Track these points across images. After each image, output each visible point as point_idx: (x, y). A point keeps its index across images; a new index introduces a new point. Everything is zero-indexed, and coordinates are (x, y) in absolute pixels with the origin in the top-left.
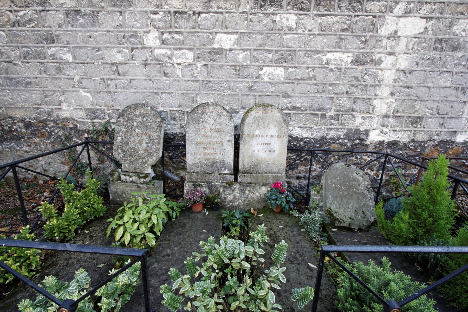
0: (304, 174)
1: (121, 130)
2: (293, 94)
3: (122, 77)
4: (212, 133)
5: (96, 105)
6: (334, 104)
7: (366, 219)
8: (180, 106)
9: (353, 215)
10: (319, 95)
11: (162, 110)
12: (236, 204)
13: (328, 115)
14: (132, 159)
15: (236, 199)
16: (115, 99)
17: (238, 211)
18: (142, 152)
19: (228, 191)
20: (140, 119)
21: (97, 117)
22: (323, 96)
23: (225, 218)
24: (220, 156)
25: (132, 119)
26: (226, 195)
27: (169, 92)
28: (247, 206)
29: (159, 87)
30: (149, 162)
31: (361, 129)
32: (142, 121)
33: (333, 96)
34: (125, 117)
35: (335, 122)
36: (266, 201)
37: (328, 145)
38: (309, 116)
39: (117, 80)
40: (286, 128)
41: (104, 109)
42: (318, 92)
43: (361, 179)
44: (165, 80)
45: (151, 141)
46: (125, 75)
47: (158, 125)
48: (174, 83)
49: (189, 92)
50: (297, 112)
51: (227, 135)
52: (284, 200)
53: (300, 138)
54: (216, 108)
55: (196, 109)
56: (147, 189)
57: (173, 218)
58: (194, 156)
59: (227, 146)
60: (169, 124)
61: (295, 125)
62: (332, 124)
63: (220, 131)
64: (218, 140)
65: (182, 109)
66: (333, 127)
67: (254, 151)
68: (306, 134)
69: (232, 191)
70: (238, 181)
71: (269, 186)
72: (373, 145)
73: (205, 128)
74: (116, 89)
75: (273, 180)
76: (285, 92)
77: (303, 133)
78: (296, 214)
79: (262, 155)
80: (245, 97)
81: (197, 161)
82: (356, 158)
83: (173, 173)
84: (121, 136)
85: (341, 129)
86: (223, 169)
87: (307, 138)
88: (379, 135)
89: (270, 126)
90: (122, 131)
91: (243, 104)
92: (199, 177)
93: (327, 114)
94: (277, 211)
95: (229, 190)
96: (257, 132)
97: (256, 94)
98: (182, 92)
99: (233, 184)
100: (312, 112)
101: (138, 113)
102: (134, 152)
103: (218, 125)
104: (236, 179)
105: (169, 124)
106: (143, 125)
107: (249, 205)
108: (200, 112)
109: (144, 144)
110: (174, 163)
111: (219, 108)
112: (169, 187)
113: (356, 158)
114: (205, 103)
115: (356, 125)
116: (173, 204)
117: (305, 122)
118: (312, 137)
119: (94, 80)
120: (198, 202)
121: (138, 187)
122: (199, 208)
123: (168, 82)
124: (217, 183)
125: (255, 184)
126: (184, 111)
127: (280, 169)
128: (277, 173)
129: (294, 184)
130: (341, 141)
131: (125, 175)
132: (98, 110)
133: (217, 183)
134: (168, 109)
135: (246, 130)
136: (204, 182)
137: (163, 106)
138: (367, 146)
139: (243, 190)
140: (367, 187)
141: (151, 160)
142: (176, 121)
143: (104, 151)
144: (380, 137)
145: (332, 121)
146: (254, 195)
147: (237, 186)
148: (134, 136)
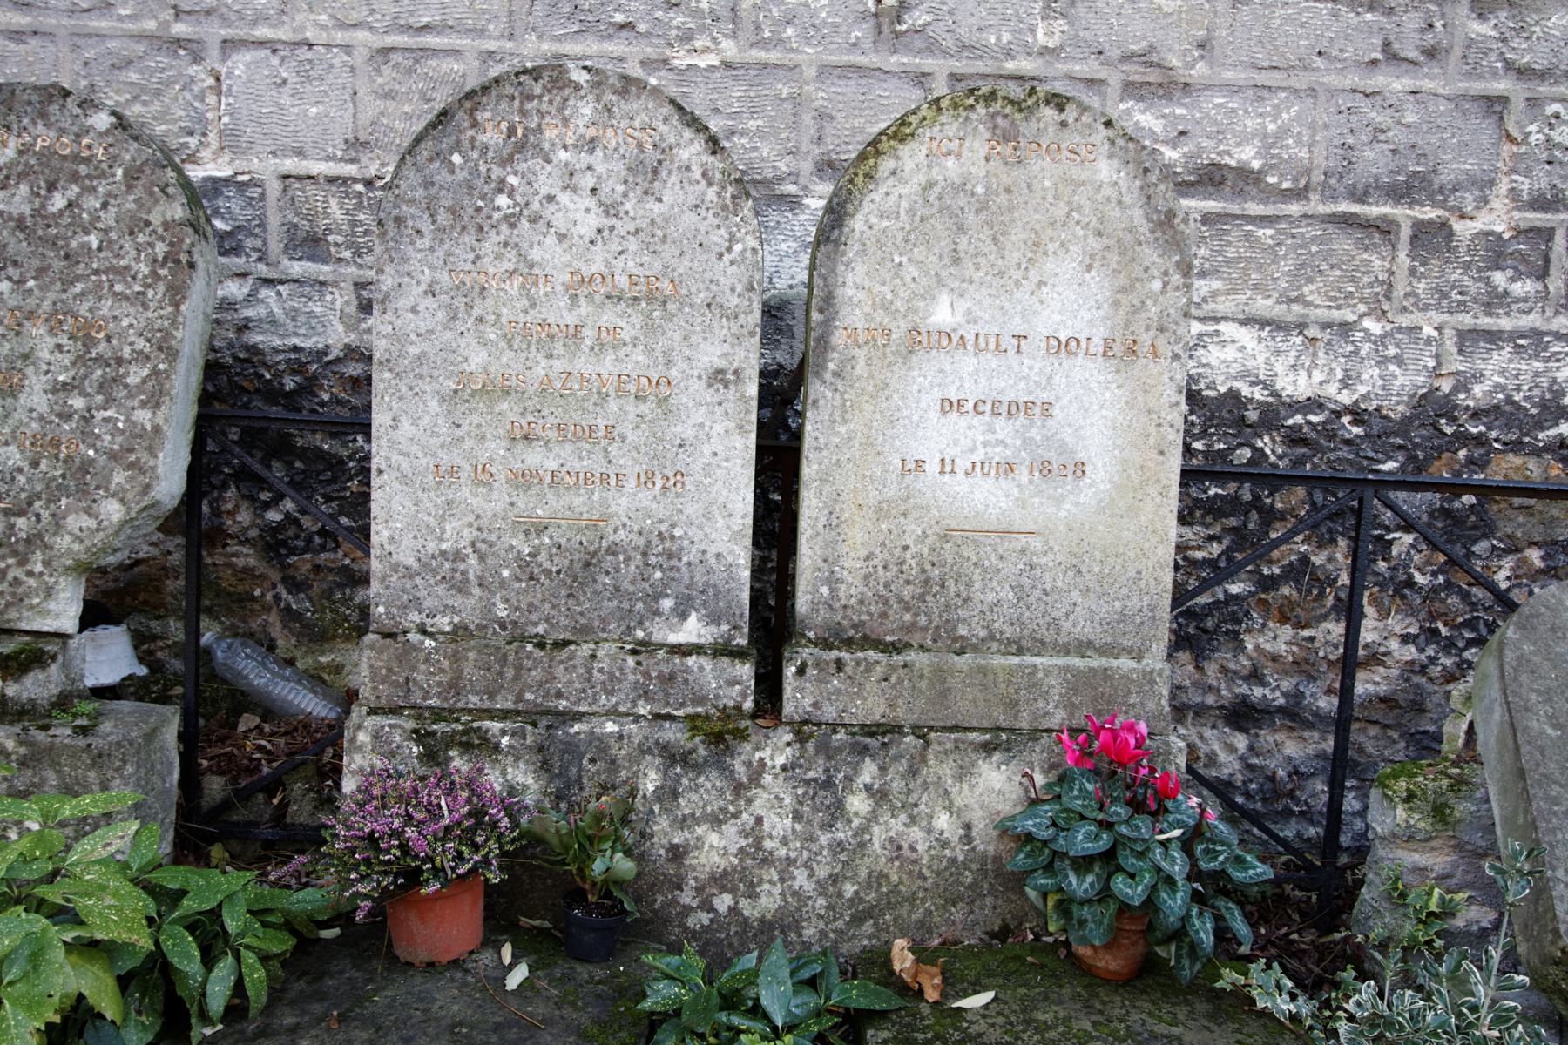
0: (1286, 685)
2: (1200, 70)
4: (585, 308)
6: (1507, 148)
10: (1396, 83)
11: (226, 172)
12: (769, 900)
13: (1463, 230)
15: (767, 861)
17: (778, 958)
19: (704, 792)
22: (1427, 85)
23: (665, 1017)
24: (645, 497)
26: (683, 823)
27: (283, 34)
28: (857, 920)
30: (63, 542)
32: (37, 213)
33: (1500, 86)
35: (1518, 288)
36: (1017, 881)
37: (1470, 461)
38: (1320, 240)
40: (1176, 279)
42: (1392, 55)
45: (98, 369)
47: (161, 249)
49: (430, 40)
50: (1234, 208)
51: (708, 329)
52: (1177, 866)
53: (1264, 408)
54: (621, 107)
55: (462, 118)
56: (23, 763)
57: (205, 1019)
58: (428, 496)
59: (699, 416)
60: (269, 282)
61: (1223, 306)
62: (1495, 301)
63: (648, 297)
64: (628, 368)
65: (373, 171)
66: (1505, 323)
67: (919, 464)
68: (1300, 378)
69: (739, 788)
70: (788, 708)
71: (1037, 755)
73: (528, 269)
75: (1071, 707)
76: (1145, 57)
77: (1279, 368)
78: (1275, 994)
79: (986, 499)
80: (849, 88)
81: (457, 534)
83: (291, 662)
86: (667, 604)
87: (1313, 404)
89: (1050, 265)
91: (830, 143)
92: (469, 671)
93: (1458, 226)
94: (1111, 963)
95: (711, 781)
96: (943, 314)
97: (928, 63)
98: (378, 42)
99: (741, 735)
100: (1345, 207)
103: (633, 245)
104: (769, 688)
105: (269, 282)
107: (869, 913)
108: (492, 136)
110: (295, 586)
111: (642, 110)
112: (227, 766)
114: (535, 73)
116: (223, 887)
117: (1296, 279)
118: (1346, 398)
120: (438, 871)
122: (449, 928)
124: (611, 727)
125: (920, 732)
127: (1123, 617)
128: (1106, 650)
133: (611, 727)
134: (265, 167)
135: (859, 287)
136: (505, 715)
137: (231, 143)
139: (828, 784)
141: (78, 522)
142: (325, 262)
145: (1499, 278)
146: (916, 834)
147: (776, 750)
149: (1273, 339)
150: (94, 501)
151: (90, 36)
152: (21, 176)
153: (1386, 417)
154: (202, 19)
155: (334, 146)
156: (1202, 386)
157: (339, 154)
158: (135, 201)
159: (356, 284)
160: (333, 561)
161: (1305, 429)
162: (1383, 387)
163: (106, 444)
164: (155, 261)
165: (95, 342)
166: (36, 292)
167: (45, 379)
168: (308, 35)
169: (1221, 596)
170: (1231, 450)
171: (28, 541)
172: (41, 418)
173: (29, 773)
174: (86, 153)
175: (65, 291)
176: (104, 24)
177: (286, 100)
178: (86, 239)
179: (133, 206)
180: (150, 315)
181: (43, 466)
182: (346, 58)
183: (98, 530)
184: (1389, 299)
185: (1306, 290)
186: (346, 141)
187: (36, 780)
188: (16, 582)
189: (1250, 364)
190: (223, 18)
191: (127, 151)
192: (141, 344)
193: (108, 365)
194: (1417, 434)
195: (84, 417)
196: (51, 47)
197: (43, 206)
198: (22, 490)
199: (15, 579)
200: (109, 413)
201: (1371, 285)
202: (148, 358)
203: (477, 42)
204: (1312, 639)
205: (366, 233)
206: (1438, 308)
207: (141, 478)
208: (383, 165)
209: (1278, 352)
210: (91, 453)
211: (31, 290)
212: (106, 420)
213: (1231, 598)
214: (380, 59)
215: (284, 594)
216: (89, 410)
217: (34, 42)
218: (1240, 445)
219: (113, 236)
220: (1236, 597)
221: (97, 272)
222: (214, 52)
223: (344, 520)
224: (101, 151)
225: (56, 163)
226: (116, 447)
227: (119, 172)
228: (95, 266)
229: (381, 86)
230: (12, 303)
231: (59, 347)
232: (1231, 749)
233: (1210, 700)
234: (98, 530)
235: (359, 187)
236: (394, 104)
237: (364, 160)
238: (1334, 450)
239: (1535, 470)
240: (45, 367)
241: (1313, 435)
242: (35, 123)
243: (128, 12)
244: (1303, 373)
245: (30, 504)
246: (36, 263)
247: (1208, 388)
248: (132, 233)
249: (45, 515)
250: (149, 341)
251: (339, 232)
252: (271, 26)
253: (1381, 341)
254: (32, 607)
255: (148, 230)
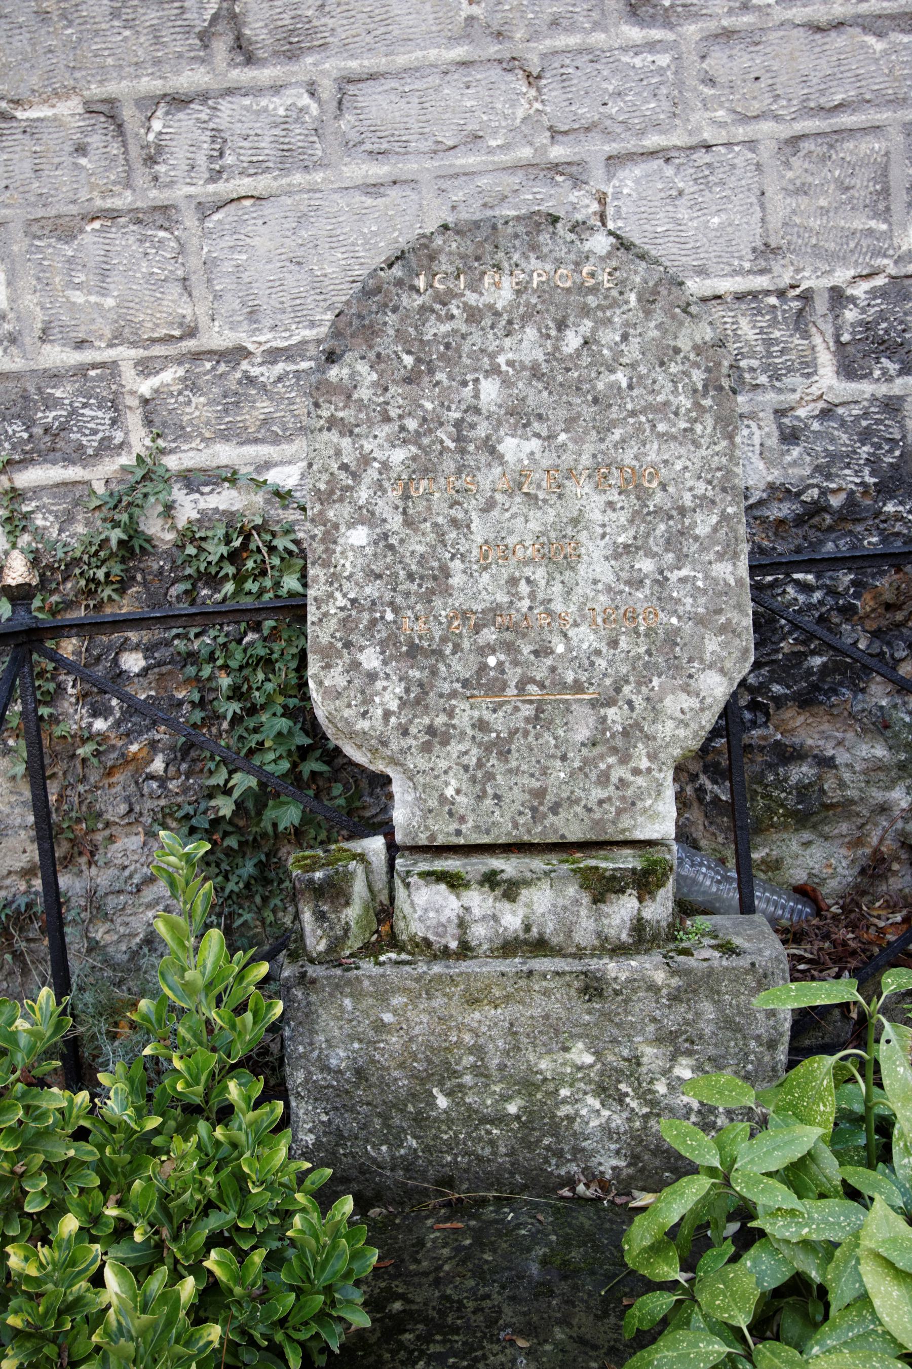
1: (366, 460)
3: (265, 74)
5: (45, 336)
8: (767, 252)
14: (498, 721)
16: (209, 264)
18: (585, 637)
20: (528, 346)
21: (51, 445)
25: (450, 349)
27: (677, 139)
29: (586, 112)
30: (666, 729)
32: (553, 356)
34: (386, 344)
39: (225, 105)
41: (111, 368)
44: (637, 49)
45: (659, 523)
46: (292, 54)
47: (698, 376)
48: (719, 61)
49: (846, 120)
56: (675, 998)
65: (786, 280)
74: (216, 176)
84: (366, 516)
90: (372, 473)
101: (500, 292)
102: (509, 647)
106: (566, 390)
109: (596, 566)
119: (31, 129)
121: (593, 988)
123: (664, 60)
126: (807, 297)
131: (454, 882)
132: (55, 376)
141: (676, 703)
143: (102, 738)
148: (490, 505)
150: (690, 676)
151: (456, 176)
152: (525, 318)
154: (582, 137)
155: (741, 258)
157: (747, 265)
158: (657, 327)
159: (776, 411)
160: (764, 738)
163: (688, 608)
164: (695, 391)
165: (650, 494)
166: (571, 446)
167: (602, 543)
168: (706, 135)
171: (625, 733)
172: (609, 589)
173: (682, 1008)
174: (591, 282)
175: (602, 440)
176: (471, 160)
177: (683, 214)
178: (613, 378)
179: (656, 333)
180: (704, 453)
181: (624, 643)
182: (750, 155)
183: (702, 710)
186: (754, 250)
187: (690, 1016)
188: (622, 783)
190: (606, 132)
191: (636, 272)
192: (701, 487)
193: (671, 517)
195: (657, 581)
196: (414, 196)
197: (557, 348)
198: (605, 675)
199: (621, 780)
200: (684, 572)
202: (713, 502)
203: (899, 114)
205: (782, 352)
207: (737, 641)
208: (797, 271)
210: (674, 620)
211: (564, 445)
212: (683, 580)
214: (788, 150)
215: (709, 785)
216: (661, 572)
217: (394, 193)
219: (643, 370)
221: (633, 413)
222: (598, 172)
223: (776, 688)
224: (606, 277)
225: (559, 298)
226: (701, 610)
227: (633, 297)
228: (629, 406)
229: (791, 181)
230: (546, 463)
231: (610, 504)
234: (702, 710)
235: (773, 300)
236: (806, 199)
237: (777, 268)
240: (600, 531)
242: (527, 258)
243: (499, 142)
245: (618, 690)
246: (562, 413)
248: (662, 364)
249: (638, 700)
250: (709, 482)
251: (752, 355)
252: (661, 132)
254: (645, 811)
255: (679, 358)
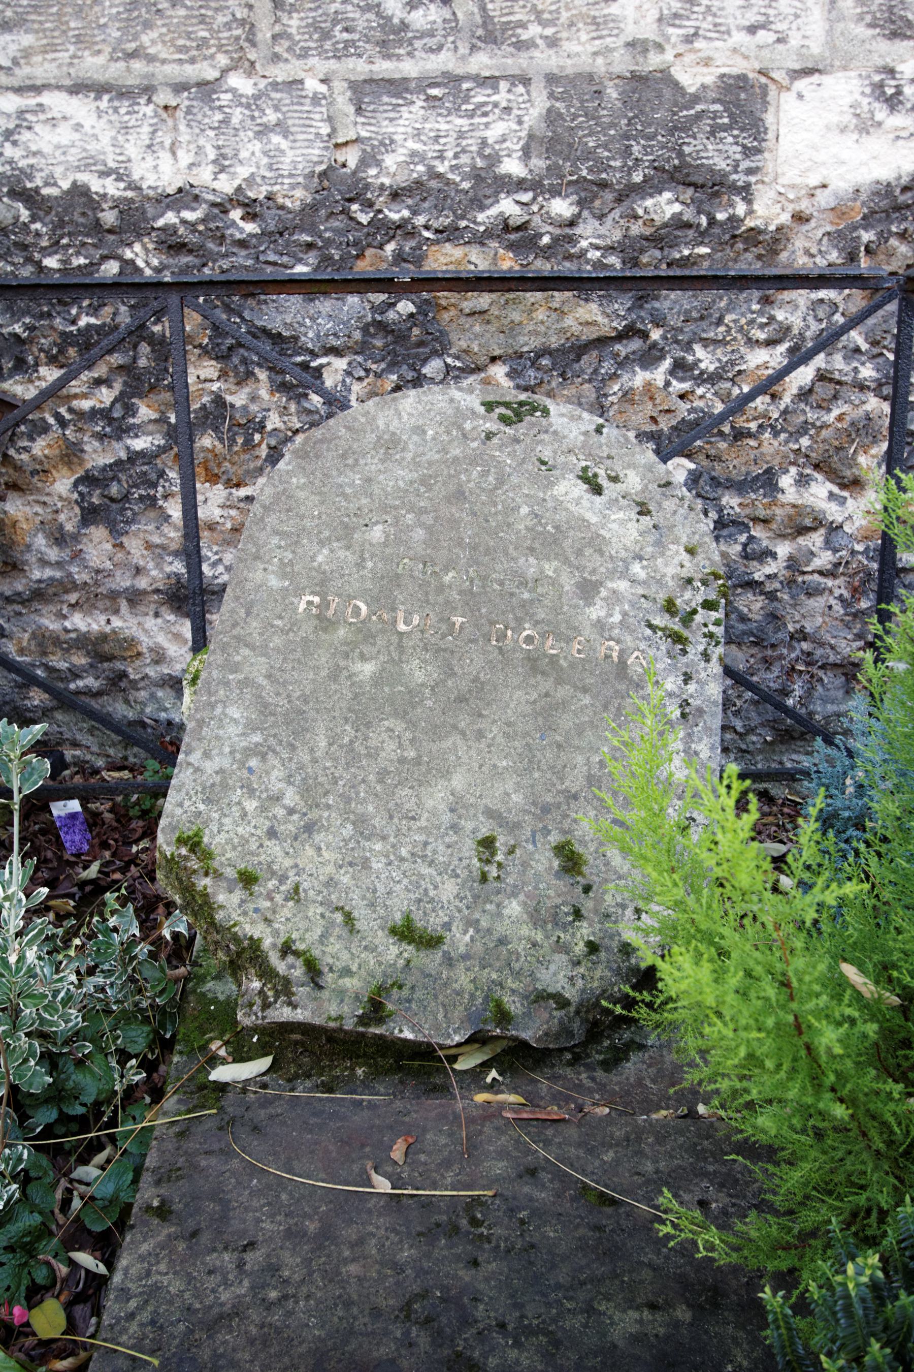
7: (585, 931)
9: (449, 889)
31: (690, 78)
43: (623, 529)
53: (124, 207)
61: (42, 69)
66: (409, 68)
68: (162, 162)
72: (819, 228)
77: (133, 150)
82: (680, 368)
85: (490, 82)
87: (186, 196)
88: (866, 126)
113: (680, 368)
115: (631, 31)
118: (226, 186)
129: (159, 657)
130: (507, 206)
138: (773, 243)
140: (670, 607)
144: (876, 143)
149: (116, 110)
153: (282, 207)
156: (39, 182)
161: (181, 231)
162: (270, 167)
169: (123, 455)
170: (93, 266)
184: (254, 44)
185: (145, 39)
189: (93, 147)
194: (328, 228)
201: (228, 26)
204: (249, 499)
206: (322, 53)
209: (125, 128)
213: (134, 457)
218: (105, 258)
220: (142, 454)
232: (177, 637)
233: (143, 583)
238: (226, 256)
239: (479, 260)
241: (193, 239)
244: (165, 156)
247: (47, 184)
253: (253, 104)
